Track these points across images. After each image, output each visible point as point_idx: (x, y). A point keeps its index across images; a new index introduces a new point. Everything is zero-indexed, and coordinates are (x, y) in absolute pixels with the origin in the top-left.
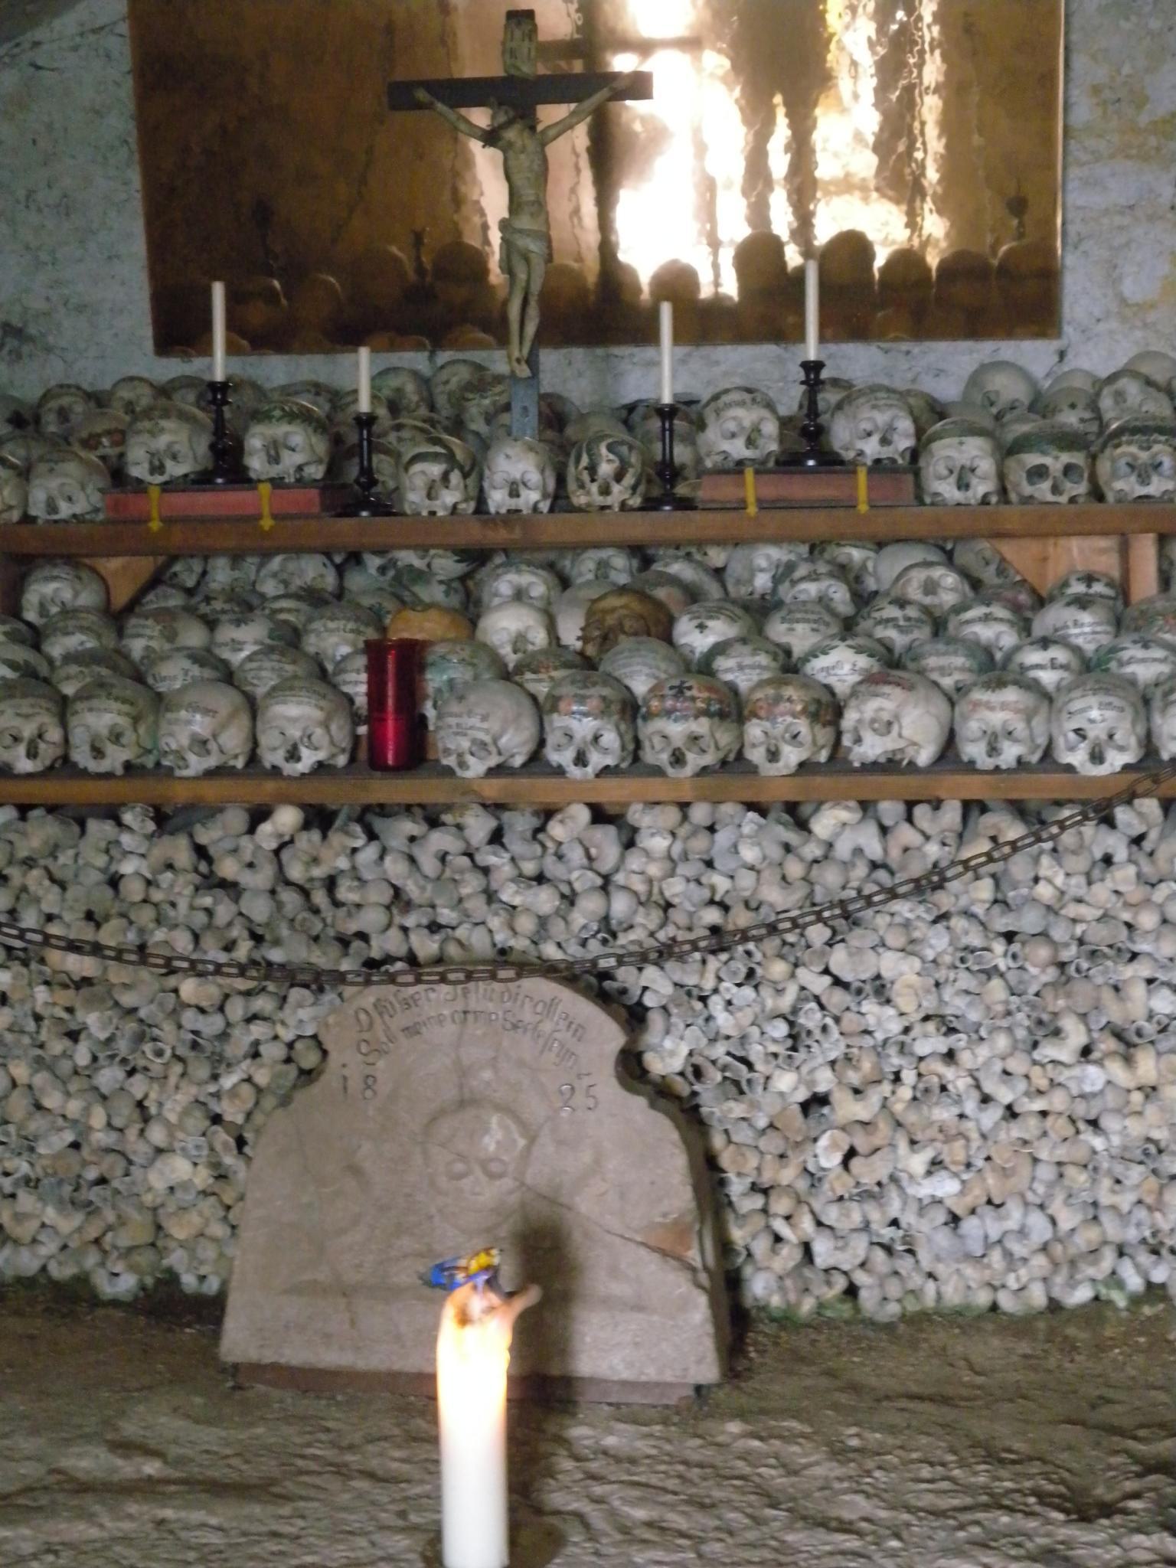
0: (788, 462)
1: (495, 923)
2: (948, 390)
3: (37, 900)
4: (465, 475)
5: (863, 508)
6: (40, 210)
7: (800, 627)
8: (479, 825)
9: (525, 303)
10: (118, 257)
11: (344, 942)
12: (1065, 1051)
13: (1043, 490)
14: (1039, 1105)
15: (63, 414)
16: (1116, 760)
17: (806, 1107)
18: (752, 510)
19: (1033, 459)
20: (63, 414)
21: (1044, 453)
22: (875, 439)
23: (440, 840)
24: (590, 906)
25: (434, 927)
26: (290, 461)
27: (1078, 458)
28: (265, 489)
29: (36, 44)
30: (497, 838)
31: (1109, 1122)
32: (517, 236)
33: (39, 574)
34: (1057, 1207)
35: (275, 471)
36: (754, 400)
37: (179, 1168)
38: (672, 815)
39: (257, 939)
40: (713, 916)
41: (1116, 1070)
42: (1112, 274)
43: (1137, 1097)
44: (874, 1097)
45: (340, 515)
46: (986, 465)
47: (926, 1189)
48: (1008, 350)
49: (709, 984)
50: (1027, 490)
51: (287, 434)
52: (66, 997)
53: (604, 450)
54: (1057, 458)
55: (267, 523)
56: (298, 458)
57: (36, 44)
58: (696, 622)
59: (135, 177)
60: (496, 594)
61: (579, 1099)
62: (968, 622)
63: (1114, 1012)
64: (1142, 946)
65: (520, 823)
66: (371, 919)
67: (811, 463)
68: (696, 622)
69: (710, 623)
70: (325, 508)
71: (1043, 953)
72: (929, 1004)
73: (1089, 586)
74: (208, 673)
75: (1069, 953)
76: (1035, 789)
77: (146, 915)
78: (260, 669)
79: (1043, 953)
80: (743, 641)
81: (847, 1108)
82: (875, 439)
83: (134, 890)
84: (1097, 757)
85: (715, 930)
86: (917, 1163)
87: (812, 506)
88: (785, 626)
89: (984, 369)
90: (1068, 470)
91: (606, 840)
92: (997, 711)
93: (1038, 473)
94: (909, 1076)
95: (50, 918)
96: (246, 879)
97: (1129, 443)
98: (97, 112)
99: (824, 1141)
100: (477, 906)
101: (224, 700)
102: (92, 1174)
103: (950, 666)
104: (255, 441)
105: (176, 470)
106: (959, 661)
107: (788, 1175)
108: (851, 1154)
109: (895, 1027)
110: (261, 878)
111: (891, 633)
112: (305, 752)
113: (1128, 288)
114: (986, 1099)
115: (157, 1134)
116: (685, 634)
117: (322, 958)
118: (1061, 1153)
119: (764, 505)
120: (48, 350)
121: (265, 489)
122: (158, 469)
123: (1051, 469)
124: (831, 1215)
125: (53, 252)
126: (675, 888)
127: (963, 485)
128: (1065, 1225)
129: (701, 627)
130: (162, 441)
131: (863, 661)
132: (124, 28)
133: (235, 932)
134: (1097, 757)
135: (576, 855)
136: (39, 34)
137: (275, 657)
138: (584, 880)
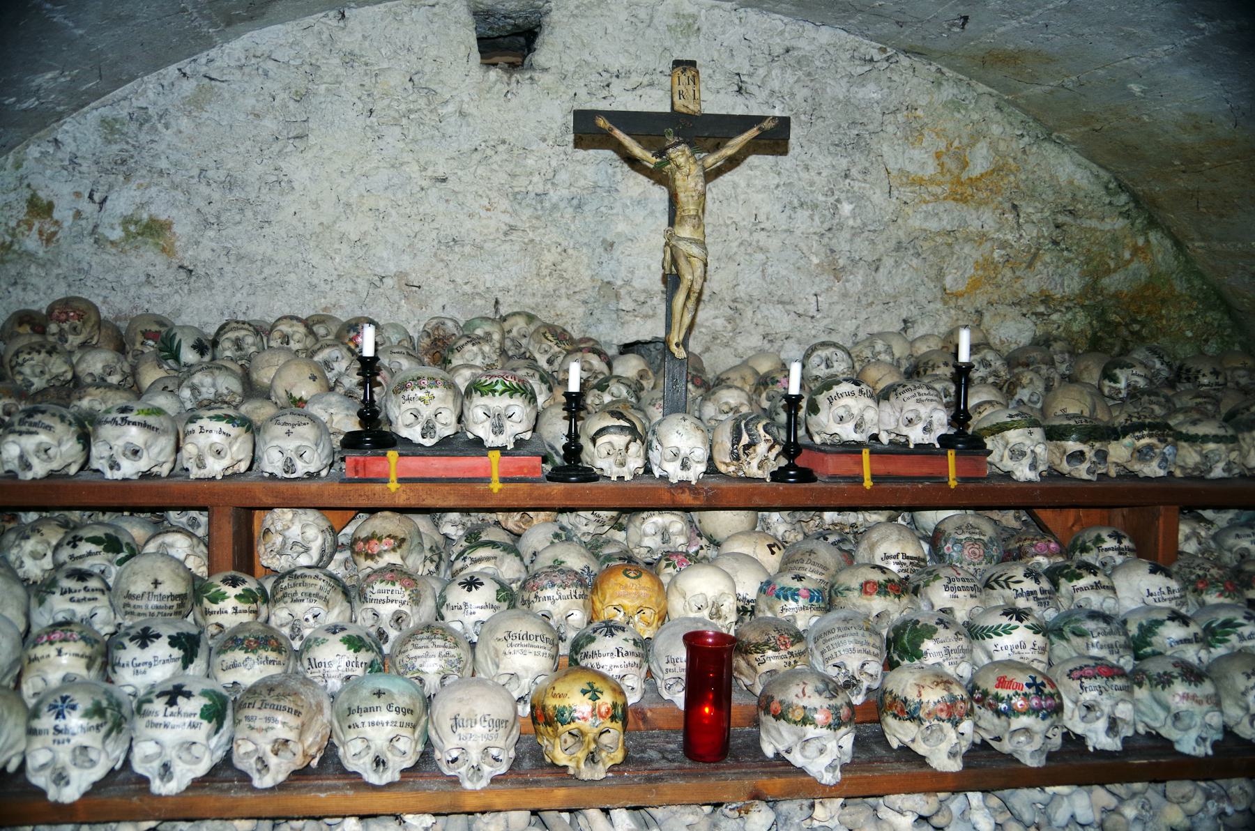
6: (209, 184)
7: (961, 594)
10: (269, 222)
15: (238, 344)
20: (238, 344)
29: (211, 61)
53: (762, 432)
57: (211, 61)
62: (1081, 589)
73: (1120, 542)
88: (950, 593)
98: (257, 116)
125: (218, 218)
136: (213, 53)
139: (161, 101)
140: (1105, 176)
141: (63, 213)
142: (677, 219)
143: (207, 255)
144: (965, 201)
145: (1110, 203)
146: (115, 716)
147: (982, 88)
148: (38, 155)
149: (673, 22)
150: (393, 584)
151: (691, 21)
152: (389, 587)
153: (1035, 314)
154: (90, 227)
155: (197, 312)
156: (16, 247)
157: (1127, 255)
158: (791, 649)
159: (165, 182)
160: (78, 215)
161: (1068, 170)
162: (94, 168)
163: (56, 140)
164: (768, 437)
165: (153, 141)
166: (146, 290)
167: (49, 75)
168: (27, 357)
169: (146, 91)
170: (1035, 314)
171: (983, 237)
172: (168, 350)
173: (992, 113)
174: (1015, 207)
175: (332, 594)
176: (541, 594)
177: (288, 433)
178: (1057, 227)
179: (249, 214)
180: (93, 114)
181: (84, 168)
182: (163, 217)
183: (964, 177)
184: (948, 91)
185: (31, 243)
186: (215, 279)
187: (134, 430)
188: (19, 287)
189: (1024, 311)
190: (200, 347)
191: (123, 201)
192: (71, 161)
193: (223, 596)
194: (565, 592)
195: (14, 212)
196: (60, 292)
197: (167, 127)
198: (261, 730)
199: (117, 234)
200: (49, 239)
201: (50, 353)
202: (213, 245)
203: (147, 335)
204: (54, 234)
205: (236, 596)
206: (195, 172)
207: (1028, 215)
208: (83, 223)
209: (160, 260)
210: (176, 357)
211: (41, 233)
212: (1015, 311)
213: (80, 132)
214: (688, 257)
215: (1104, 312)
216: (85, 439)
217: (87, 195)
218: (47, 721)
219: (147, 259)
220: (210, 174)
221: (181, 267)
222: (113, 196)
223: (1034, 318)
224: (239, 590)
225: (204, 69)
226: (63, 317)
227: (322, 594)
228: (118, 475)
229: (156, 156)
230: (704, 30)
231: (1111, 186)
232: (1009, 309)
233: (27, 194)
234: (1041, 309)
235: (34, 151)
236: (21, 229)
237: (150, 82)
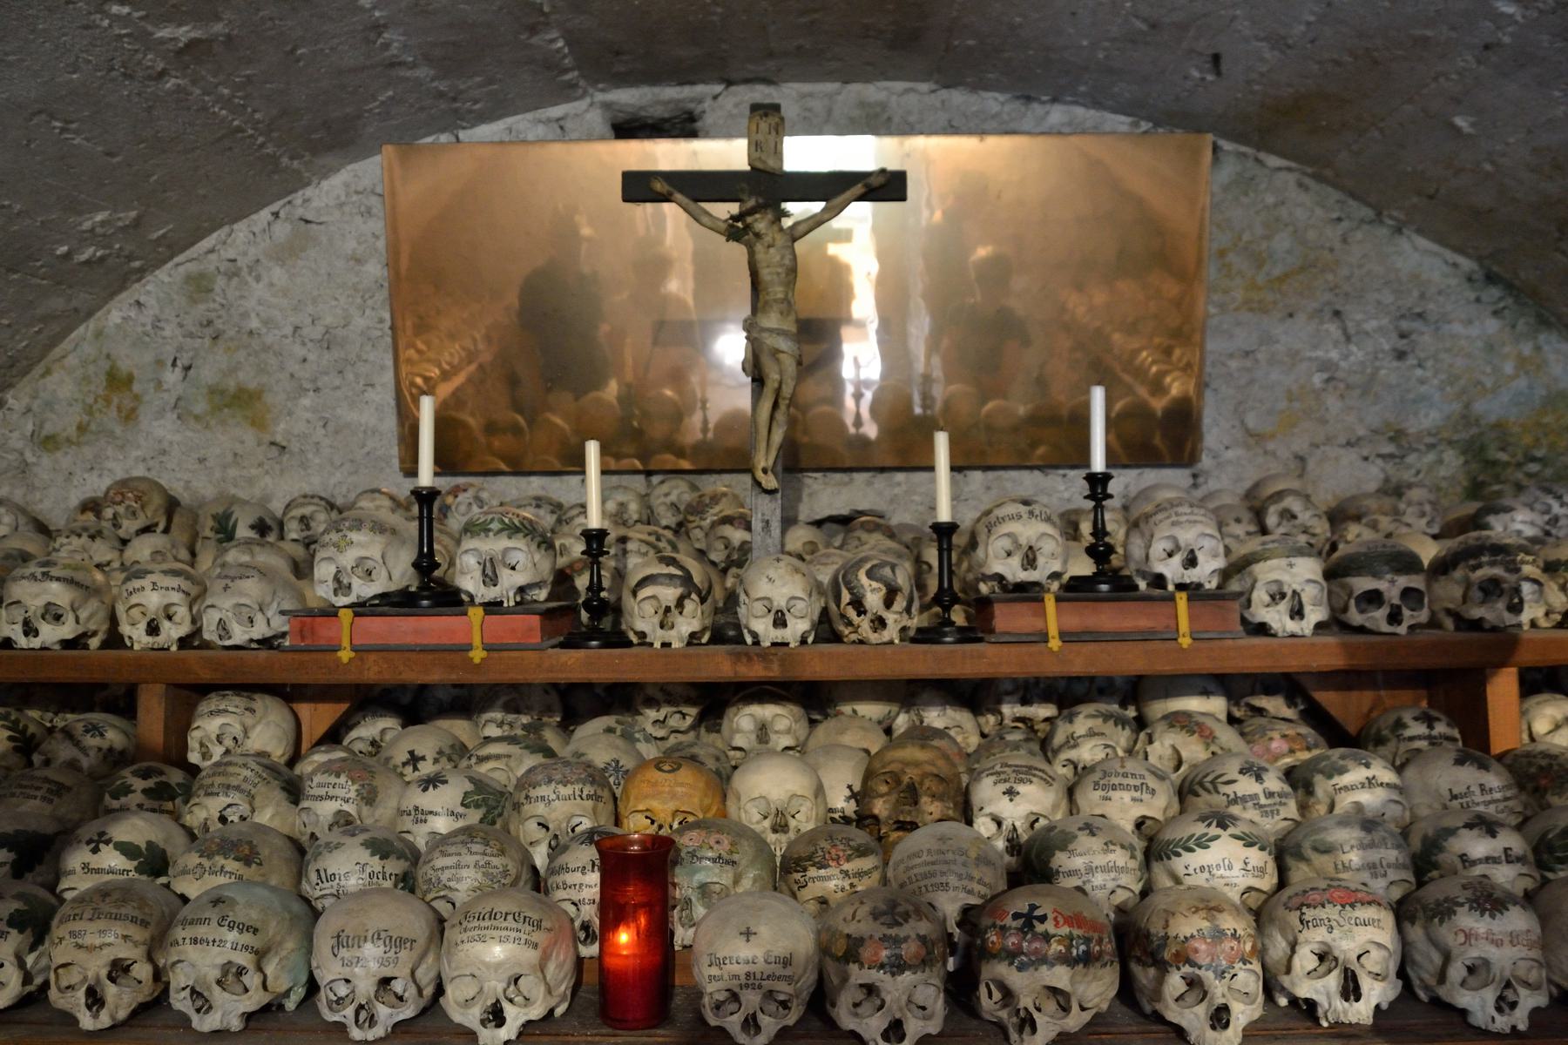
4: (703, 600)
6: (304, 344)
9: (775, 406)
10: (372, 385)
13: (1377, 618)
15: (304, 520)
19: (1363, 584)
21: (1376, 575)
22: (1177, 559)
26: (509, 582)
28: (476, 614)
29: (306, 201)
32: (765, 335)
33: (204, 707)
35: (491, 594)
36: (1031, 513)
45: (562, 645)
51: (506, 551)
54: (1392, 582)
55: (477, 655)
56: (521, 579)
57: (306, 201)
58: (1004, 787)
60: (738, 731)
62: (1346, 788)
67: (1104, 587)
68: (1004, 787)
69: (1021, 788)
70: (546, 633)
73: (1431, 727)
78: (458, 866)
82: (1177, 559)
87: (1120, 637)
90: (1407, 593)
93: (1373, 598)
97: (1492, 564)
98: (359, 261)
105: (364, 589)
112: (509, 1011)
116: (991, 801)
119: (1065, 636)
121: (476, 614)
123: (1386, 596)
125: (314, 380)
129: (1011, 793)
130: (348, 558)
136: (309, 192)
137: (476, 848)
139: (252, 251)
140: (1467, 264)
142: (760, 305)
143: (300, 427)
144: (1265, 311)
145: (1478, 300)
147: (1273, 161)
148: (119, 321)
149: (856, 113)
150: (338, 776)
151: (878, 109)
152: (332, 779)
153: (1379, 456)
154: (173, 401)
155: (280, 489)
156: (93, 427)
157: (1509, 368)
158: (846, 866)
162: (178, 331)
163: (138, 303)
164: (875, 584)
165: (242, 297)
166: (233, 472)
167: (99, 217)
168: (65, 541)
170: (1379, 456)
171: (1294, 355)
172: (225, 532)
173: (1294, 194)
174: (1337, 313)
175: (262, 788)
176: (533, 793)
177: (226, 588)
178: (1403, 336)
179: (350, 376)
181: (167, 333)
182: (252, 385)
183: (1261, 279)
184: (1229, 170)
186: (310, 456)
187: (55, 586)
188: (96, 473)
189: (1365, 453)
192: (155, 327)
193: (127, 790)
194: (565, 791)
195: (92, 388)
197: (258, 279)
198: (91, 949)
199: (200, 407)
201: (92, 537)
202: (308, 415)
204: (133, 410)
205: (144, 791)
206: (288, 330)
207: (1358, 324)
208: (165, 396)
209: (249, 436)
211: (119, 409)
212: (1352, 456)
214: (775, 352)
215: (1483, 448)
217: (169, 363)
220: (305, 331)
221: (273, 443)
223: (1379, 461)
224: (150, 783)
225: (300, 212)
226: (119, 498)
227: (245, 786)
228: (36, 643)
229: (245, 315)
230: (896, 120)
231: (1475, 276)
232: (1342, 451)
234: (1389, 449)
236: (99, 406)
237: (241, 230)
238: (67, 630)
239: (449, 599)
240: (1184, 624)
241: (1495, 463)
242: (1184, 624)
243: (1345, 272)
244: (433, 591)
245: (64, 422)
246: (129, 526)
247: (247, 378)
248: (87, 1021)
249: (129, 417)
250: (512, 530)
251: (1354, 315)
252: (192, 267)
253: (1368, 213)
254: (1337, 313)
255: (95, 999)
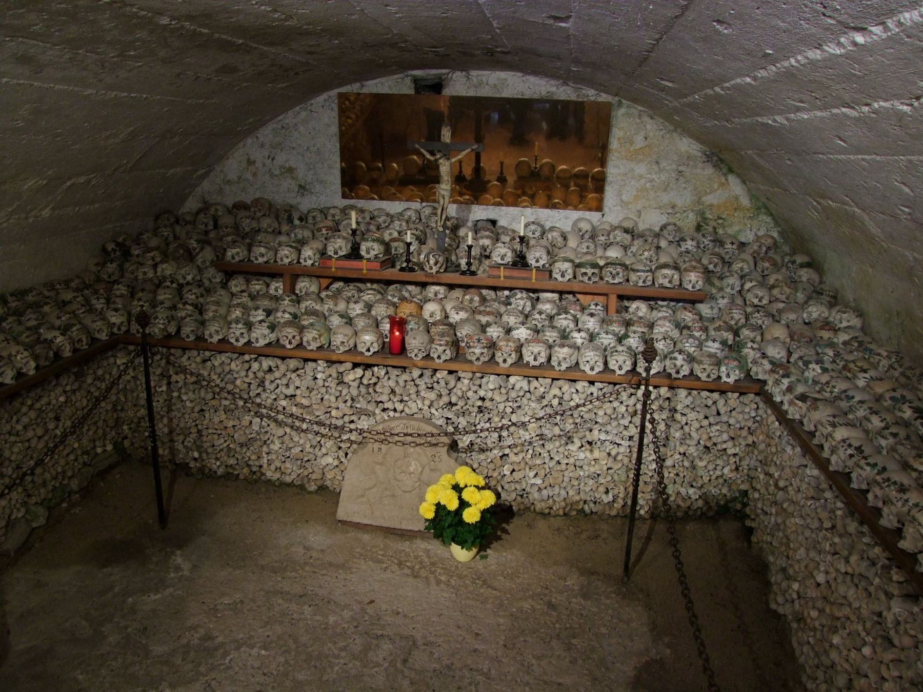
0: (515, 264)
1: (419, 402)
2: (567, 227)
3: (294, 382)
5: (534, 281)
8: (416, 373)
11: (378, 403)
12: (573, 448)
14: (566, 461)
15: (314, 218)
16: (597, 370)
17: (501, 457)
18: (502, 279)
19: (583, 270)
23: (405, 377)
24: (445, 399)
25: (401, 401)
26: (373, 253)
27: (596, 271)
28: (365, 261)
30: (421, 376)
31: (585, 467)
33: (300, 280)
34: (568, 489)
37: (329, 460)
38: (470, 375)
39: (353, 400)
40: (479, 403)
41: (588, 454)
42: (620, 194)
43: (593, 463)
44: (521, 456)
46: (570, 271)
47: (533, 481)
48: (588, 215)
49: (477, 422)
50: (581, 278)
52: (300, 411)
55: (365, 272)
59: (338, 145)
61: (437, 459)
63: (589, 437)
64: (599, 420)
65: (428, 373)
66: (384, 398)
71: (571, 421)
72: (538, 432)
74: (344, 320)
75: (578, 421)
76: (573, 375)
77: (324, 390)
79: (571, 421)
80: (496, 323)
81: (513, 458)
83: (320, 382)
84: (592, 369)
85: (479, 407)
86: (532, 474)
87: (518, 278)
89: (580, 220)
90: (593, 273)
91: (452, 380)
92: (562, 353)
93: (585, 274)
94: (531, 452)
95: (297, 388)
96: (351, 383)
99: (506, 467)
100: (414, 396)
101: (349, 331)
102: (306, 459)
103: (551, 336)
104: (363, 247)
106: (555, 334)
107: (495, 474)
108: (514, 470)
109: (528, 437)
110: (355, 384)
111: (536, 323)
113: (624, 197)
114: (552, 458)
115: (324, 450)
117: (371, 407)
118: (571, 474)
119: (505, 277)
120: (312, 193)
121: (365, 261)
122: (336, 253)
124: (506, 486)
126: (470, 394)
127: (563, 276)
128: (571, 493)
131: (529, 332)
132: (336, 101)
133: (347, 398)
134: (592, 369)
135: (442, 383)
136: (312, 102)
138: (444, 392)
141: (259, 164)
146: (249, 326)
157: (716, 186)
159: (295, 152)
160: (264, 165)
161: (687, 146)
169: (289, 118)
171: (641, 177)
172: (290, 220)
180: (271, 126)
182: (294, 166)
185: (248, 176)
190: (301, 219)
191: (281, 158)
193: (284, 300)
196: (258, 195)
199: (277, 172)
200: (255, 175)
203: (286, 211)
210: (292, 222)
213: (266, 133)
216: (250, 251)
218: (234, 325)
219: (288, 183)
222: (276, 157)
233: (246, 157)
234: (670, 211)
235: (249, 141)
238: (265, 259)
239: (360, 257)
240: (534, 277)
241: (706, 219)
242: (534, 277)
243: (662, 148)
244: (354, 253)
245: (232, 176)
246: (259, 214)
247: (292, 163)
248: (289, 346)
249: (255, 175)
250: (374, 241)
251: (663, 164)
252: (275, 126)
253: (672, 128)
254: (657, 163)
255: (290, 343)
